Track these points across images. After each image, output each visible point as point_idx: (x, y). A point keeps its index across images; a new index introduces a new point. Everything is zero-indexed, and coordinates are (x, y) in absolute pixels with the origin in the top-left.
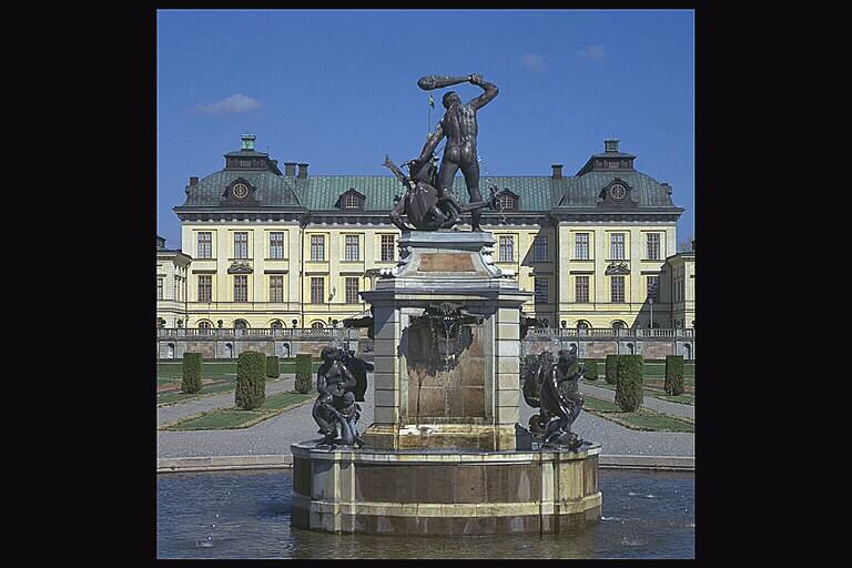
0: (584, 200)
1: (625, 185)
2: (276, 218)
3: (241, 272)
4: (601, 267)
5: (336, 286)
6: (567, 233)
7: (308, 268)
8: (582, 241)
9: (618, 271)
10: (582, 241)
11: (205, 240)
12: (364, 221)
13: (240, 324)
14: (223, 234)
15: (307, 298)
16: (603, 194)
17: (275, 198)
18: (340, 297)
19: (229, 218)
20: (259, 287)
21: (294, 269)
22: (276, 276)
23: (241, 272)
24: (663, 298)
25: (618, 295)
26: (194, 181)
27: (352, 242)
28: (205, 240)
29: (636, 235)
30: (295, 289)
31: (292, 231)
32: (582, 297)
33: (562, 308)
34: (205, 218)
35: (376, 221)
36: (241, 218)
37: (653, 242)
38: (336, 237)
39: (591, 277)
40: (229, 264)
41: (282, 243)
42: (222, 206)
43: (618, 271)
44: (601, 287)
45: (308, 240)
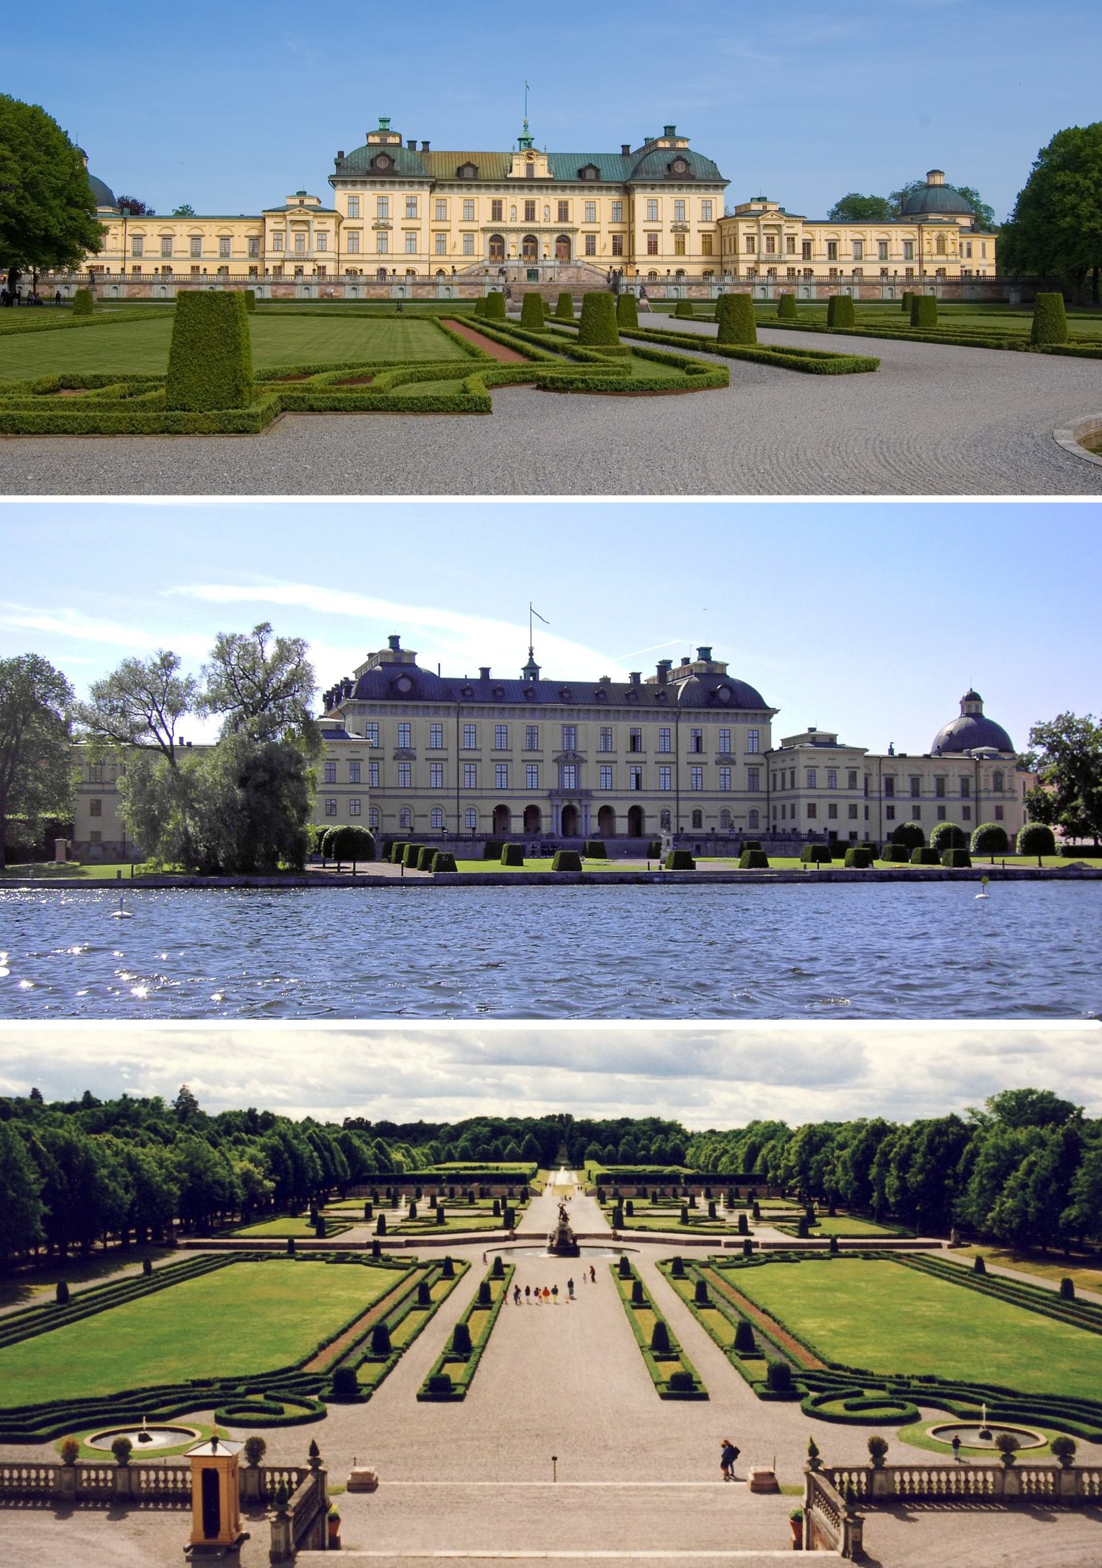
0: (654, 173)
1: (685, 161)
2: (411, 183)
3: (382, 227)
4: (667, 226)
5: (455, 240)
6: (641, 199)
8: (653, 206)
9: (680, 230)
10: (653, 206)
11: (354, 202)
12: (479, 187)
13: (382, 272)
14: (368, 197)
16: (669, 167)
17: (410, 169)
18: (460, 250)
19: (373, 183)
20: (397, 241)
22: (411, 232)
23: (382, 227)
24: (715, 250)
25: (680, 247)
26: (341, 154)
27: (469, 206)
28: (354, 202)
29: (694, 201)
30: (425, 242)
31: (423, 196)
32: (653, 249)
34: (354, 183)
35: (488, 187)
36: (383, 183)
37: (707, 207)
38: (455, 200)
39: (659, 234)
40: (373, 223)
41: (415, 205)
42: (368, 174)
43: (680, 230)
44: (667, 243)
45: (433, 201)
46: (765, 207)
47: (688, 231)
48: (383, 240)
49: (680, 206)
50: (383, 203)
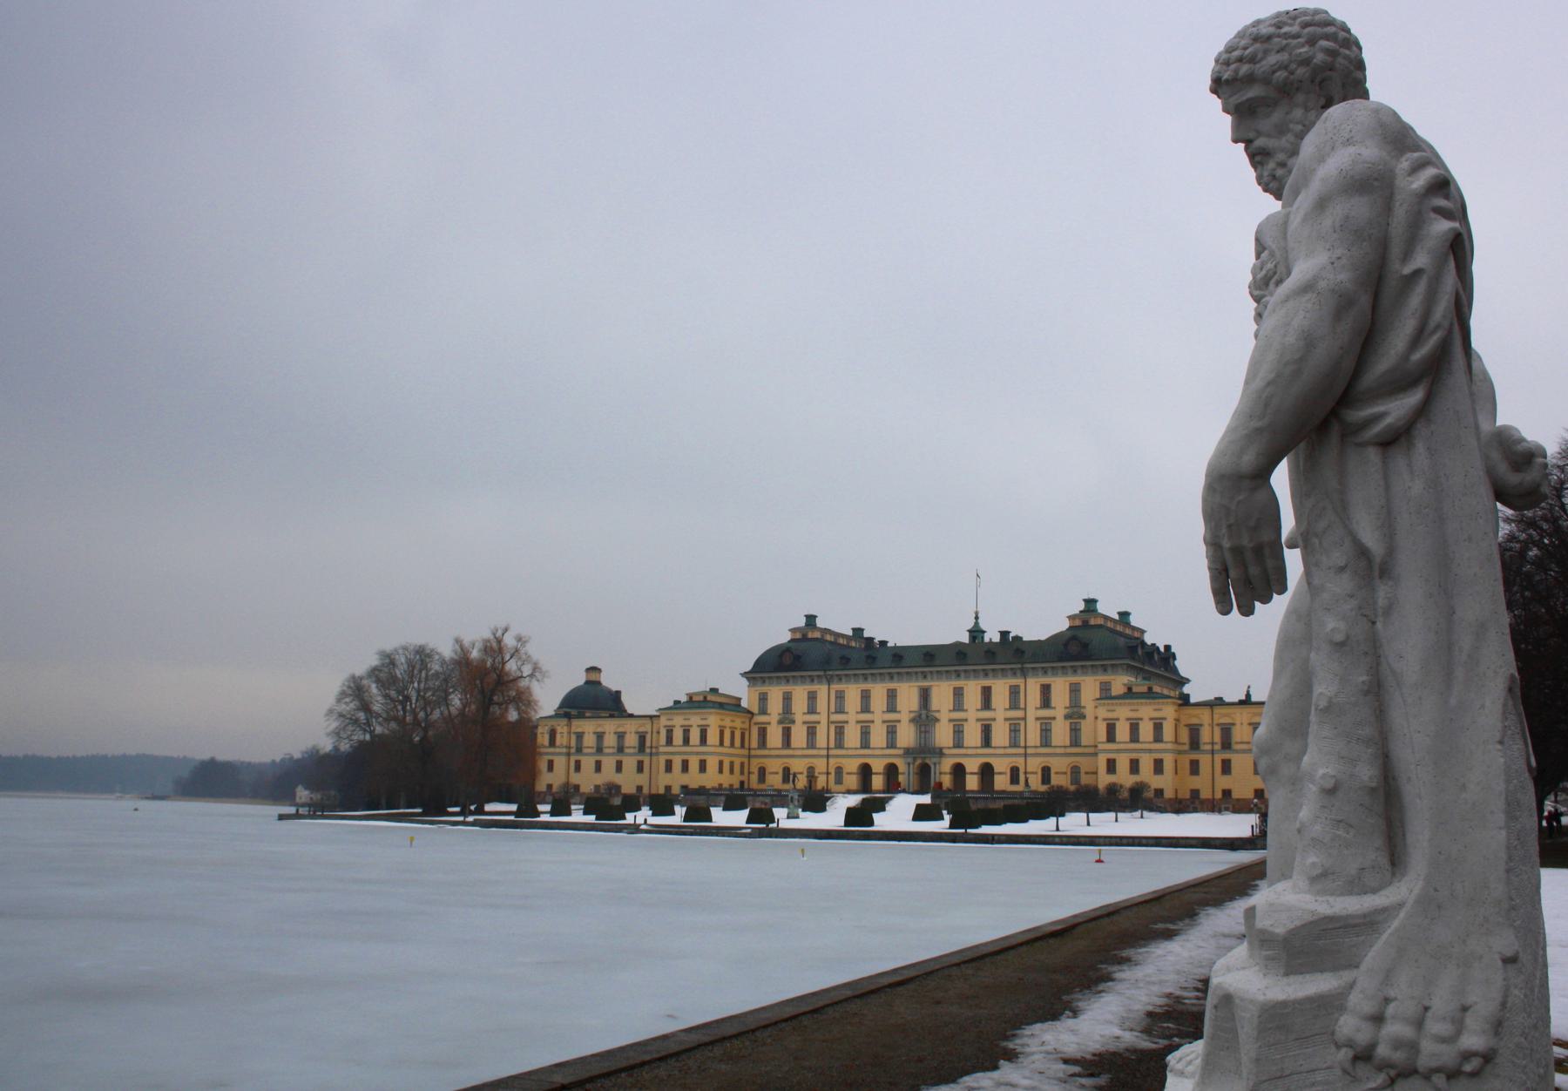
3: (787, 718)
7: (835, 717)
8: (1046, 690)
9: (1075, 714)
14: (775, 694)
15: (832, 745)
20: (799, 736)
21: (823, 718)
31: (822, 690)
32: (1046, 740)
33: (1029, 751)
46: (1150, 689)
47: (1084, 717)
48: (787, 734)
49: (1075, 690)
50: (787, 698)
